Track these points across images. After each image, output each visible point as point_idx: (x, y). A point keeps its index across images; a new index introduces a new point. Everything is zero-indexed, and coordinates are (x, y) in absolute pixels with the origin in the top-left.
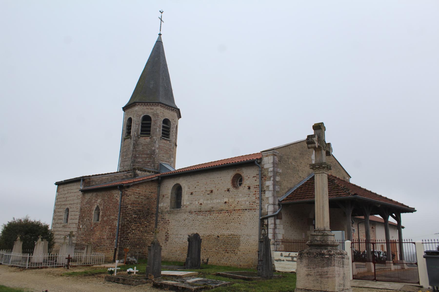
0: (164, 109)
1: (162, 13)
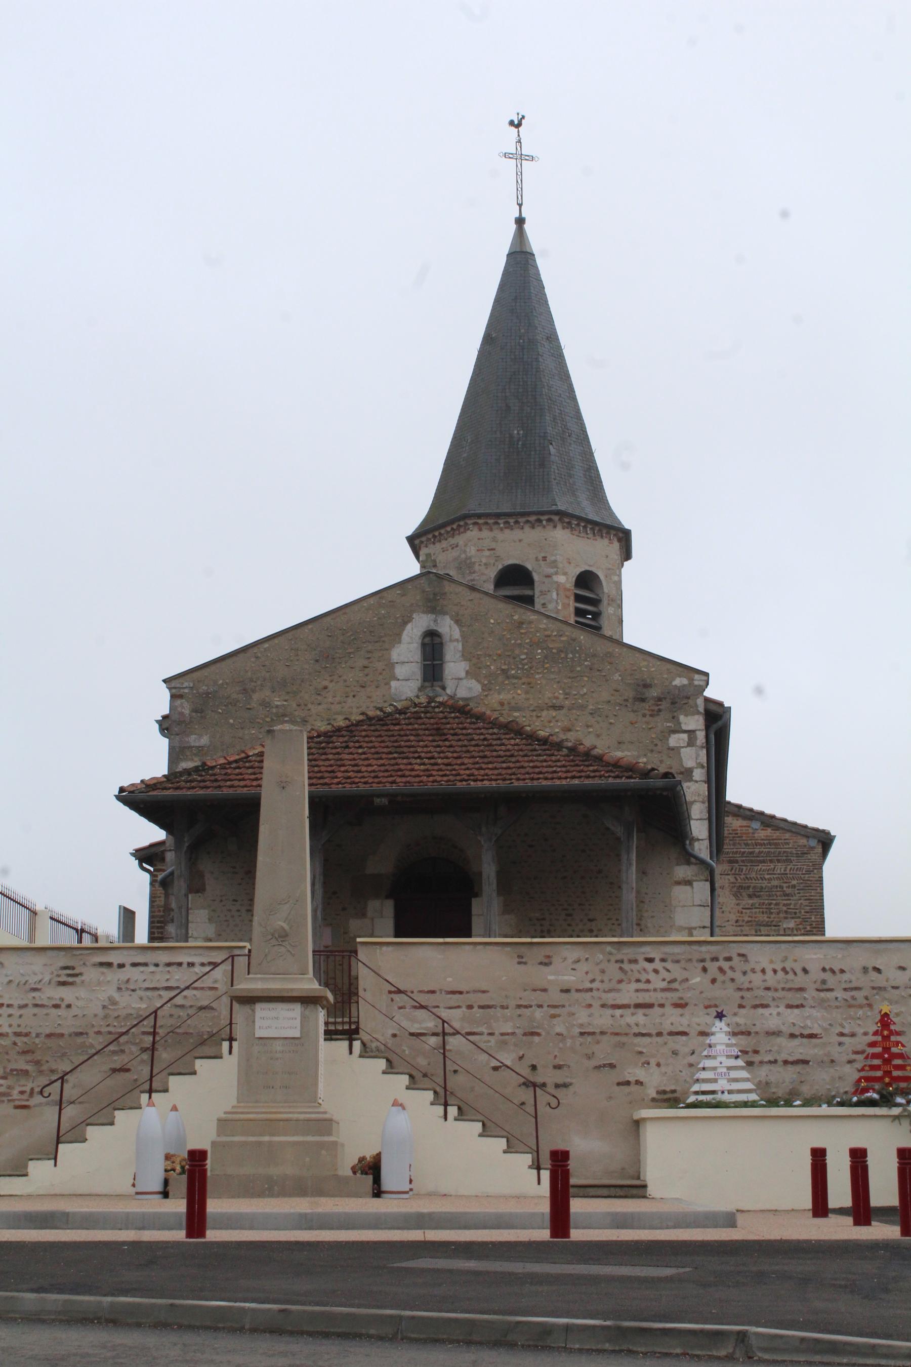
0: (496, 533)
1: (518, 125)
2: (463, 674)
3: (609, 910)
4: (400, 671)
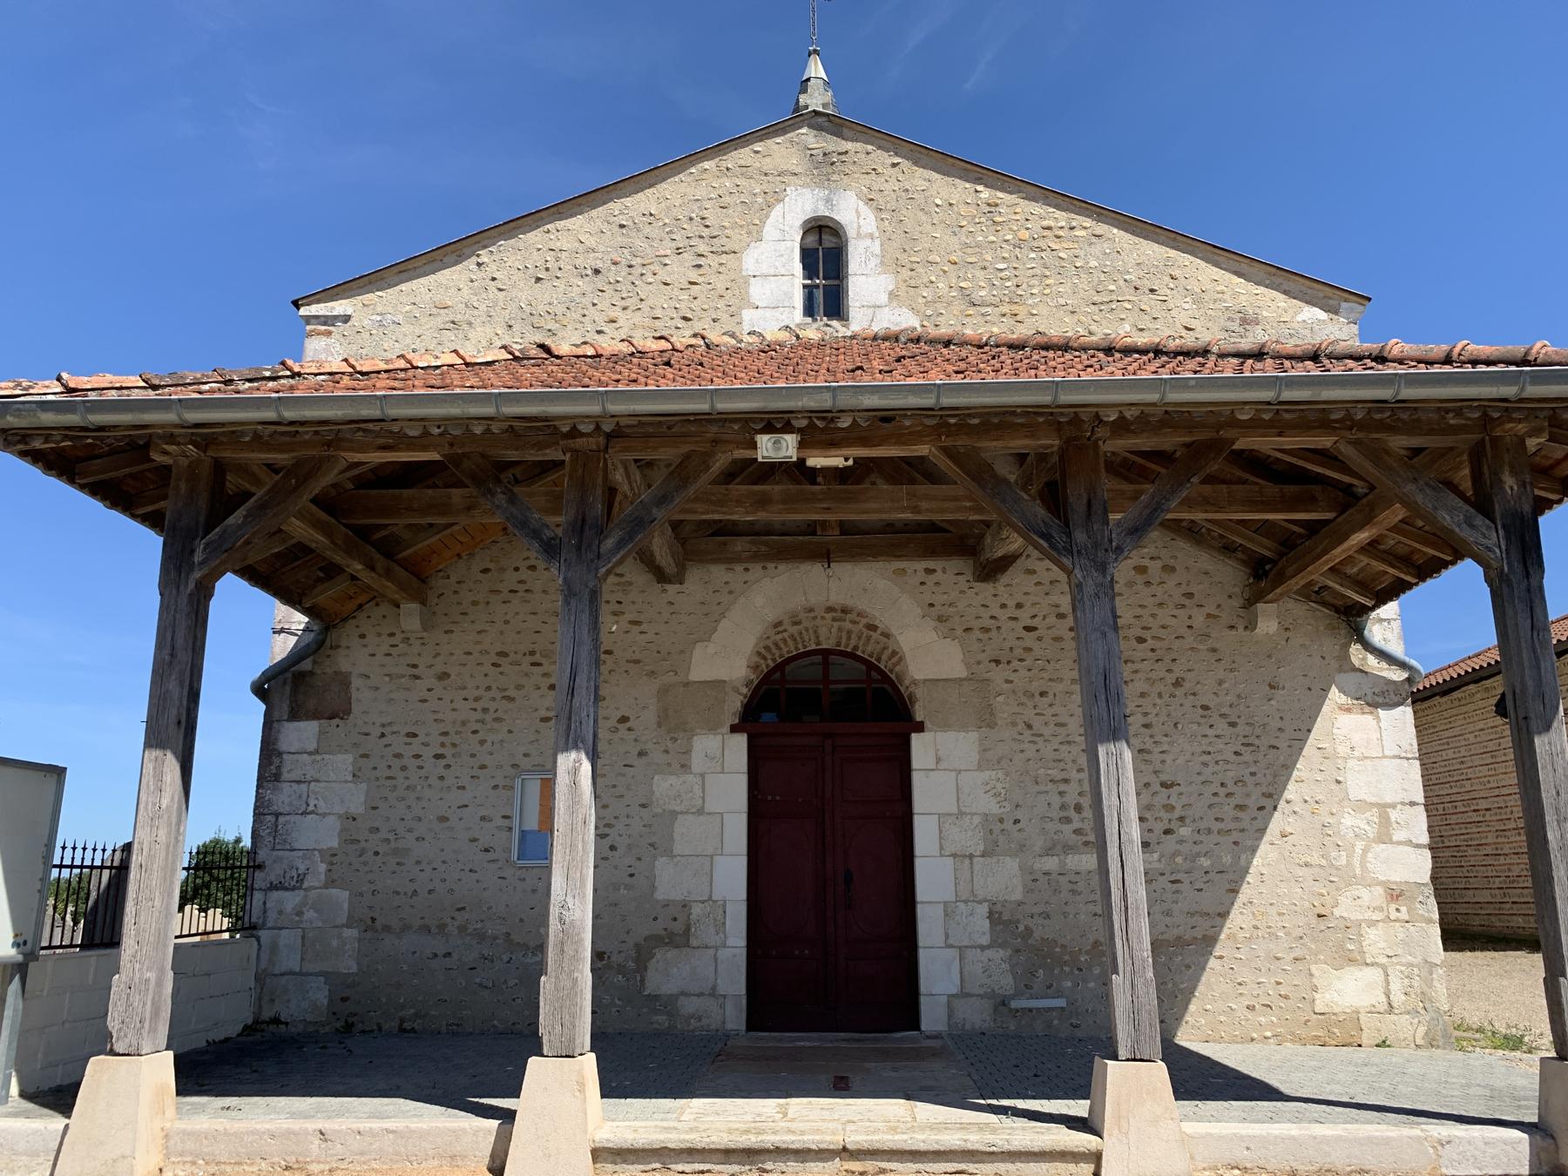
2: (884, 298)
3: (1205, 764)
4: (757, 291)
